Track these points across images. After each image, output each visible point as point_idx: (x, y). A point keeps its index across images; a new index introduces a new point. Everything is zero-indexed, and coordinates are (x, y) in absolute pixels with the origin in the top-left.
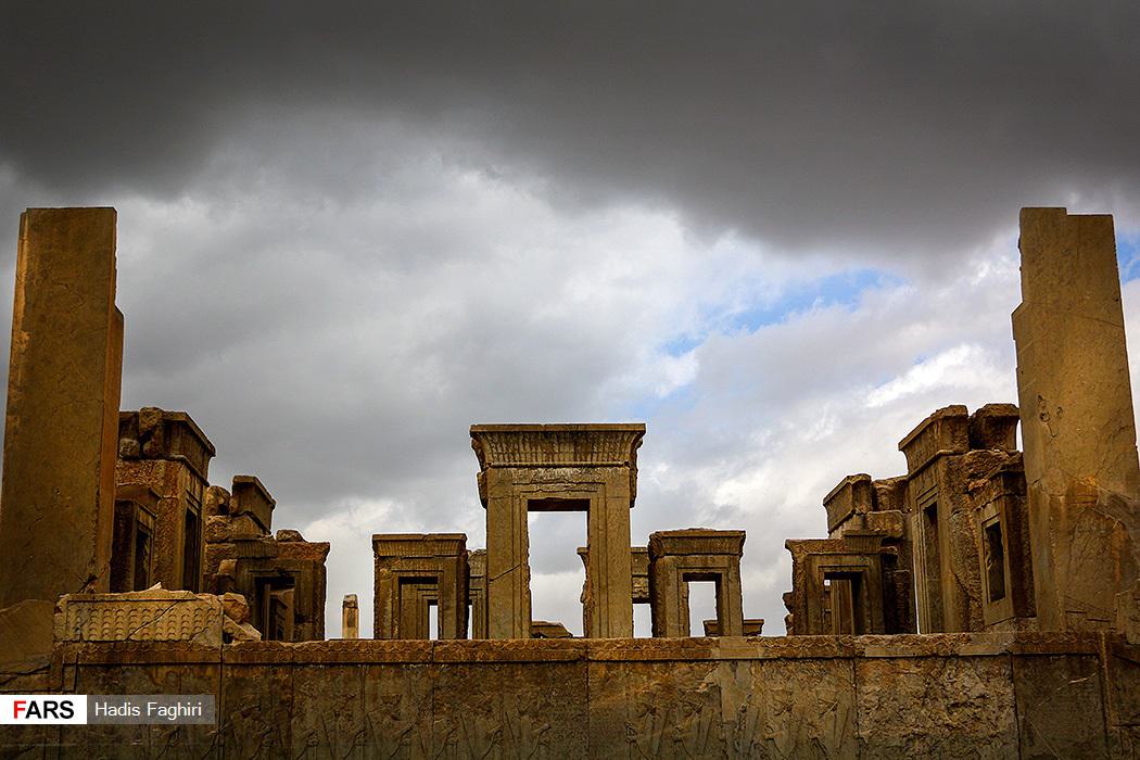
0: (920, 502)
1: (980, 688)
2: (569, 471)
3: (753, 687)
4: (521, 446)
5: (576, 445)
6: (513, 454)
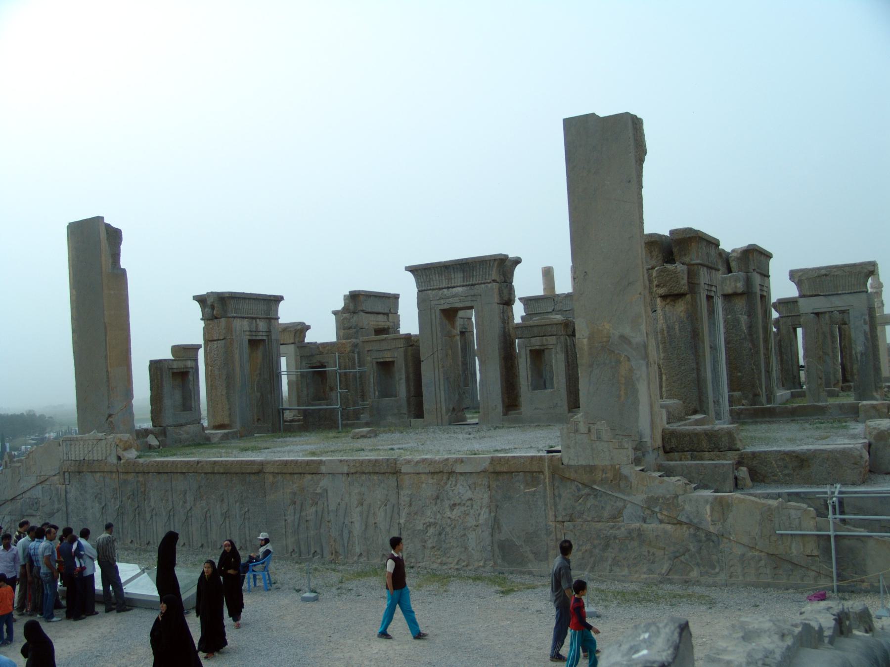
1: (469, 494)
2: (460, 289)
5: (463, 272)
6: (430, 281)
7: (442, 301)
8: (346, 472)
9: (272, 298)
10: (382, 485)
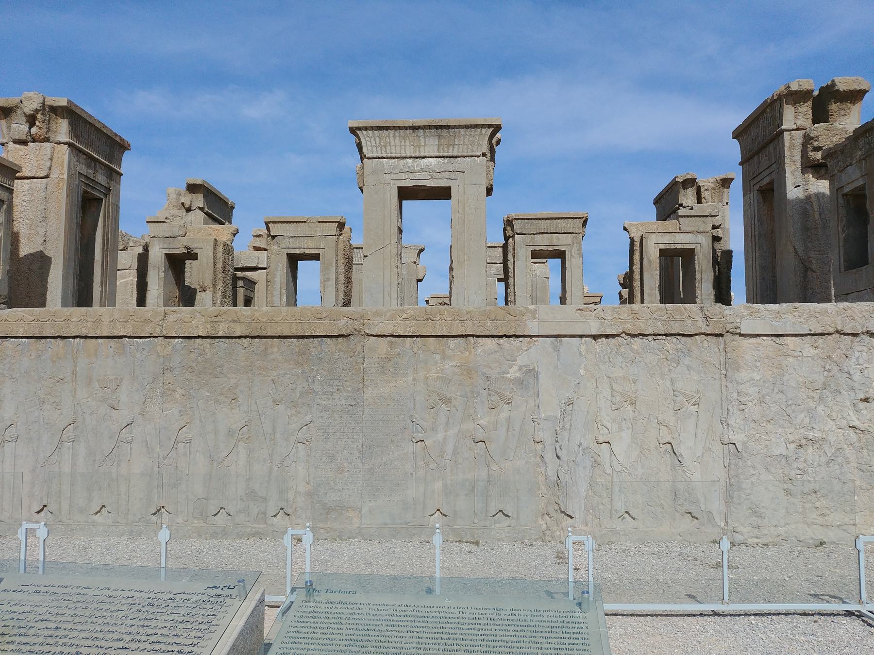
0: (753, 183)
3: (582, 372)
4: (392, 139)
5: (439, 137)
7: (403, 176)
8: (594, 332)
9: (117, 139)
10: (687, 361)
